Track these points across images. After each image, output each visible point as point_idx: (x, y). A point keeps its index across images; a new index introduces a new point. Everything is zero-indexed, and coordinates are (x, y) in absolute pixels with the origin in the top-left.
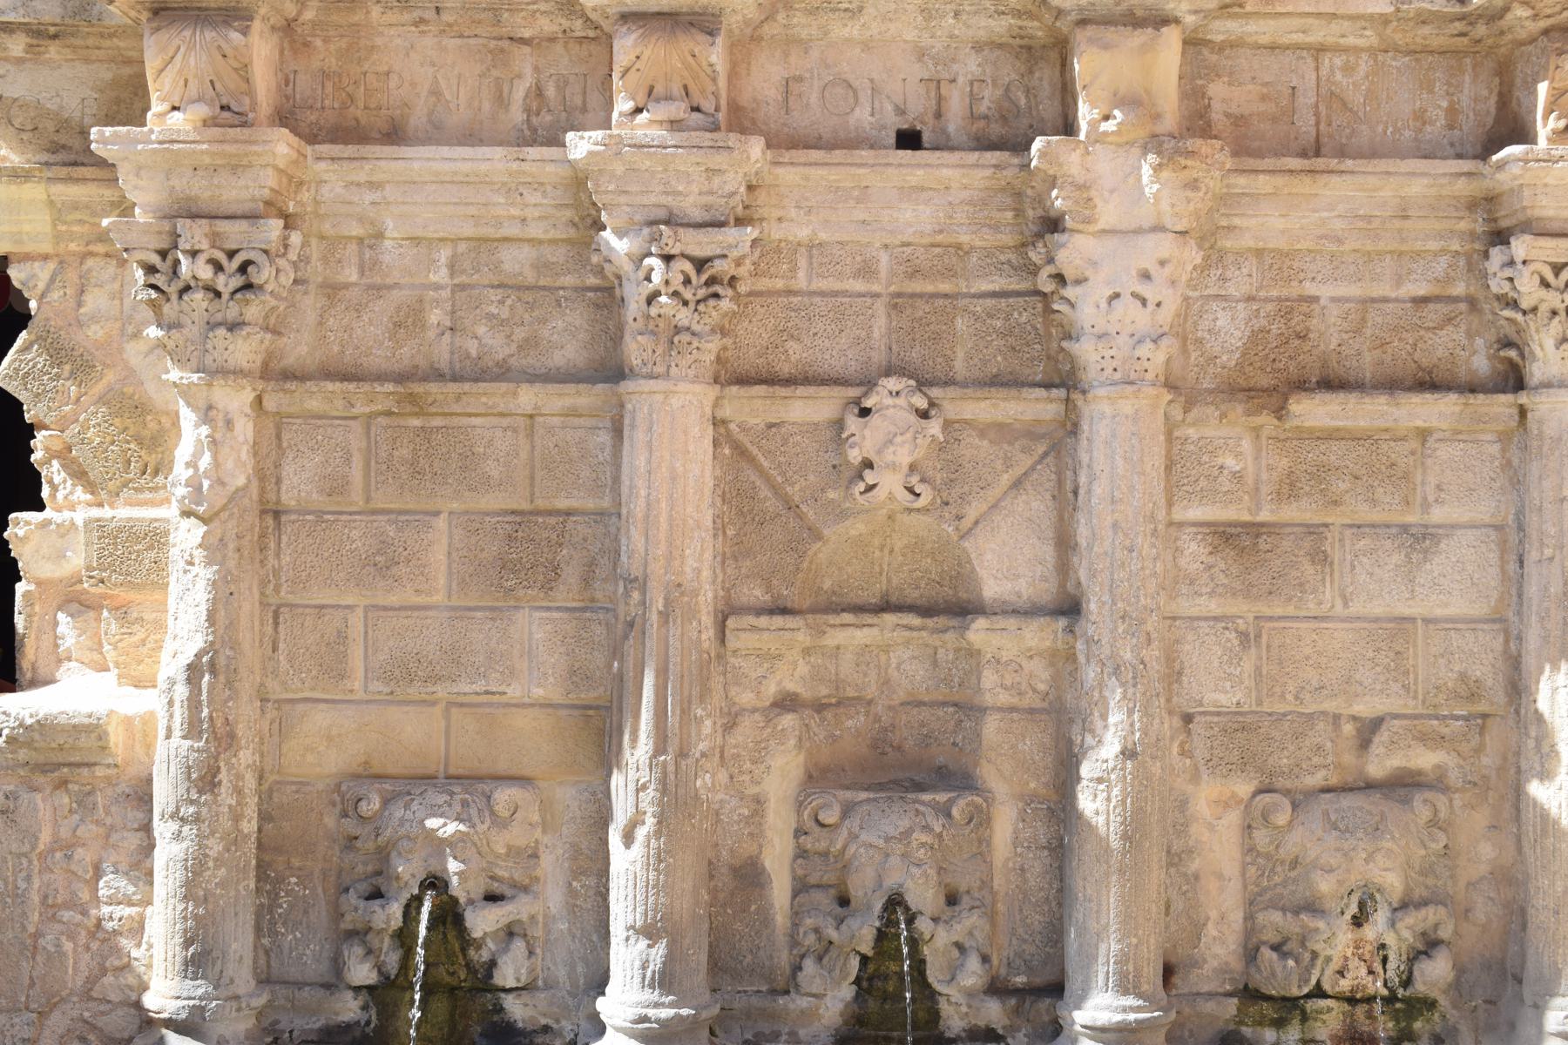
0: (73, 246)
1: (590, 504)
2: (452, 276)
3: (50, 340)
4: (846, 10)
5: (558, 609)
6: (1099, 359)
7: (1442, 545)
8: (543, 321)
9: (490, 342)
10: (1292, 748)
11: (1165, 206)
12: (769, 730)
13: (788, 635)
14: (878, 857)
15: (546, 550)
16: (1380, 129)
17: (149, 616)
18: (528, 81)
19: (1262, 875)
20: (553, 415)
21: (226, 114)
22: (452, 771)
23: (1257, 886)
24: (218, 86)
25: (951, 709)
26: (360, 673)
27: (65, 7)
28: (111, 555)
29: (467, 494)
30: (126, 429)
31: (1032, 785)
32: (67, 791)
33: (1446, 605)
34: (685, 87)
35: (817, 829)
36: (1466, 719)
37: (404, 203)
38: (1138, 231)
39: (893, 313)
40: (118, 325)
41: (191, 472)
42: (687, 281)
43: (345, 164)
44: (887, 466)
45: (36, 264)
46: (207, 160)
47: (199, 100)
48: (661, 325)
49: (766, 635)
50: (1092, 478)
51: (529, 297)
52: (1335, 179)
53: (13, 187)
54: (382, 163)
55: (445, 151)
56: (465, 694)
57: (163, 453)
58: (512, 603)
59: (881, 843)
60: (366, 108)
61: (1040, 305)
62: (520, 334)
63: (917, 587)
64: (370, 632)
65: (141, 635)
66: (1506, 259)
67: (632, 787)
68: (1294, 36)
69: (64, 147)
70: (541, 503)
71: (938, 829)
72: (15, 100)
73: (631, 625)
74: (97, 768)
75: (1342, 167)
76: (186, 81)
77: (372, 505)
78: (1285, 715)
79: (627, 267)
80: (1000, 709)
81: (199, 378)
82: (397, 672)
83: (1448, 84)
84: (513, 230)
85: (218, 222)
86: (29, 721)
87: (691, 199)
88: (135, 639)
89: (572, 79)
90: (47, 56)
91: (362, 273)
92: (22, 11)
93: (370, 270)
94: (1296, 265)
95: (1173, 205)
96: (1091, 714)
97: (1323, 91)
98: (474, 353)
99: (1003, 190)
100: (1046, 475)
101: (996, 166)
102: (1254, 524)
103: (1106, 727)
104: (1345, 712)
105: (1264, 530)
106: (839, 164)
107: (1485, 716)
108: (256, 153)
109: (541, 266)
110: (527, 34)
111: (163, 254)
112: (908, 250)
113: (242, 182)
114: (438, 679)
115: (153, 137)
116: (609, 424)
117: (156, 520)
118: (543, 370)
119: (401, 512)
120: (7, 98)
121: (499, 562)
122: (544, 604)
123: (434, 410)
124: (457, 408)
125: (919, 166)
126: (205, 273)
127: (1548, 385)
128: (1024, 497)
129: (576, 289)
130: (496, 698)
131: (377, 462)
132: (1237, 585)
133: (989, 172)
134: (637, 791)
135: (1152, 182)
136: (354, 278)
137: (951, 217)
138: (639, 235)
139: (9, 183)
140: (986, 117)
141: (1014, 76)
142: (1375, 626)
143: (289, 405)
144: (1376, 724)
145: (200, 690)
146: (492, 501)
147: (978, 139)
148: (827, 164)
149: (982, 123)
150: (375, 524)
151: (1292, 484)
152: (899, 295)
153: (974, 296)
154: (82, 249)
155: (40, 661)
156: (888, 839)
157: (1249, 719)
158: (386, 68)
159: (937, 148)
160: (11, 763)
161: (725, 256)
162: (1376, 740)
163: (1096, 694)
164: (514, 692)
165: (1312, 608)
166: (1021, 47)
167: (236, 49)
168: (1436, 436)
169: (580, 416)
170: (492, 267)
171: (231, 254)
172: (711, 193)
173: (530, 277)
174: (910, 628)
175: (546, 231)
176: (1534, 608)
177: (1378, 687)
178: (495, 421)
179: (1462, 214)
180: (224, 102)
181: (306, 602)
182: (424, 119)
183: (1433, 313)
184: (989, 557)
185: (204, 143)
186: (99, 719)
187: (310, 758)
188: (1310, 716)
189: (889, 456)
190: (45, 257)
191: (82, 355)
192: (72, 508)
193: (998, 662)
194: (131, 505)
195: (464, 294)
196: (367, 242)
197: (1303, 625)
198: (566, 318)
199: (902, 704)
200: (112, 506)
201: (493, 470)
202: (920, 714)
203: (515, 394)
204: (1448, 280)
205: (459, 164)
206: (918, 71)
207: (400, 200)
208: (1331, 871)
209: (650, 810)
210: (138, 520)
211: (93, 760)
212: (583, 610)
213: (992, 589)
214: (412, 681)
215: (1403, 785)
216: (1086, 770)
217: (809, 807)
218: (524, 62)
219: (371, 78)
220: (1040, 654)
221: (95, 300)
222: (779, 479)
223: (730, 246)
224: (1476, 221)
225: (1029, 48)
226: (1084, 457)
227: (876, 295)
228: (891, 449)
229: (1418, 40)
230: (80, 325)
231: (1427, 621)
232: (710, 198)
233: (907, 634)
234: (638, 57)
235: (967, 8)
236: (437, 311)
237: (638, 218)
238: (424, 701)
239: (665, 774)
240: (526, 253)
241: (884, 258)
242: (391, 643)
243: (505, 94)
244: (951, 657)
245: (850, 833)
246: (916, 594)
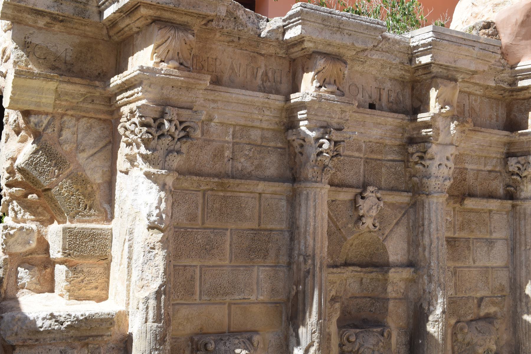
0: (60, 111)
1: (278, 227)
2: (233, 138)
3: (47, 150)
4: (362, 61)
5: (267, 266)
6: (435, 184)
7: (495, 245)
8: (263, 158)
9: (246, 165)
10: (464, 308)
11: (455, 138)
12: (332, 309)
13: (342, 274)
14: (371, 352)
15: (264, 244)
16: (482, 119)
17: (85, 270)
19: (459, 349)
20: (268, 194)
21: (182, 67)
22: (232, 330)
23: (458, 352)
24: (180, 55)
25: (368, 299)
26: (198, 293)
27: (75, 10)
28: (74, 243)
29: (239, 222)
30: (78, 190)
31: (401, 324)
32: (87, 348)
33: (496, 263)
34: (335, 80)
35: (348, 343)
36: (501, 297)
37: (224, 109)
38: (446, 145)
39: (366, 164)
40: (75, 145)
41: (158, 211)
43: (209, 92)
44: (370, 216)
45: (43, 116)
46: (180, 84)
47: (172, 59)
48: (320, 164)
49: (336, 275)
50: (430, 223)
51: (259, 149)
52: (480, 133)
53: (44, 82)
54: (222, 93)
55: (244, 92)
56: (236, 299)
57: (93, 200)
58: (251, 264)
59: (372, 347)
60: (208, 71)
61: (403, 165)
62: (256, 162)
63: (357, 258)
64: (203, 276)
65: (82, 278)
66: (517, 161)
67: (309, 333)
68: (466, 89)
69: (57, 68)
70: (263, 226)
71: (383, 341)
72: (37, 45)
73: (308, 272)
74: (104, 337)
75: (481, 130)
76: (169, 51)
77: (205, 226)
78: (462, 297)
79: (313, 142)
80: (392, 299)
81: (165, 172)
82: (213, 292)
83: (496, 108)
84: (257, 124)
85: (180, 110)
86: (81, 318)
87: (335, 120)
88: (79, 279)
89: (277, 71)
90: (53, 28)
91: (203, 134)
92: (57, 9)
93: (206, 133)
94: (464, 158)
95: (457, 137)
96: (432, 299)
97: (470, 106)
98: (240, 169)
99: (400, 127)
101: (402, 119)
102: (455, 238)
103: (437, 304)
104: (474, 296)
105: (456, 240)
106: (361, 113)
107: (505, 296)
108: (201, 84)
109: (263, 138)
110: (263, 52)
111: (155, 120)
112: (371, 144)
113: (190, 95)
114: (226, 294)
115: (163, 72)
116: (285, 198)
117: (94, 229)
118: (263, 177)
119: (214, 229)
120: (33, 44)
121: (249, 249)
122: (262, 264)
123: (229, 189)
124: (237, 189)
125: (382, 116)
127: (526, 199)
128: (400, 228)
129: (274, 147)
130: (245, 301)
131: (207, 209)
132: (451, 257)
133: (400, 121)
134: (312, 334)
135: (454, 130)
136: (200, 136)
137: (386, 134)
138: (319, 131)
139: (44, 80)
140: (392, 102)
141: (399, 90)
142: (482, 269)
143: (177, 184)
144: (481, 300)
145: (160, 302)
146: (246, 225)
147: (390, 109)
148: (358, 112)
149: (391, 104)
150: (206, 233)
151: (463, 226)
152: (367, 158)
153: (386, 161)
154: (63, 112)
155: (8, 289)
156: (374, 345)
157: (454, 299)
158: (214, 57)
160: (64, 337)
161: (343, 141)
162: (482, 304)
163: (434, 293)
164: (253, 298)
165: (467, 264)
166: (401, 81)
167: (190, 41)
168: (494, 212)
169: (276, 194)
170: (247, 136)
171: (181, 123)
172: (342, 119)
173: (259, 142)
174: (357, 272)
175: (268, 126)
176: (524, 264)
177: (483, 288)
178: (249, 195)
179: (501, 147)
180: (181, 61)
181: (179, 264)
182: (228, 78)
183: (493, 175)
184: (390, 247)
185: (182, 77)
186: (113, 316)
187: (180, 328)
188: (468, 298)
189: (371, 214)
190: (47, 114)
191: (61, 157)
192: (24, 221)
193: (393, 283)
194: (80, 222)
195: (238, 146)
196: (205, 122)
197: (466, 269)
198: (271, 158)
199: (350, 298)
200: (71, 222)
201: (248, 213)
202: (357, 301)
203: (258, 185)
204: (495, 166)
205: (248, 97)
206: (374, 84)
207: (223, 108)
208: (481, 346)
209: (316, 341)
210: (86, 228)
211: (101, 334)
212: (276, 266)
213: (392, 258)
214: (218, 295)
215: (489, 318)
216: (431, 318)
217: (346, 336)
218: (262, 62)
219: (210, 59)
220: (403, 280)
221: (66, 134)
222: (335, 220)
223: (347, 138)
224: (505, 149)
225: (403, 82)
226: (426, 216)
227: (361, 158)
228: (372, 211)
229: (491, 95)
230: (60, 144)
231: (492, 268)
232: (341, 120)
233: (356, 273)
234: (324, 68)
236: (228, 152)
237: (318, 125)
238: (221, 303)
239: (321, 326)
240: (258, 133)
241: (364, 145)
242: (211, 280)
243: (255, 73)
244: (368, 281)
245: (360, 343)
246: (356, 259)
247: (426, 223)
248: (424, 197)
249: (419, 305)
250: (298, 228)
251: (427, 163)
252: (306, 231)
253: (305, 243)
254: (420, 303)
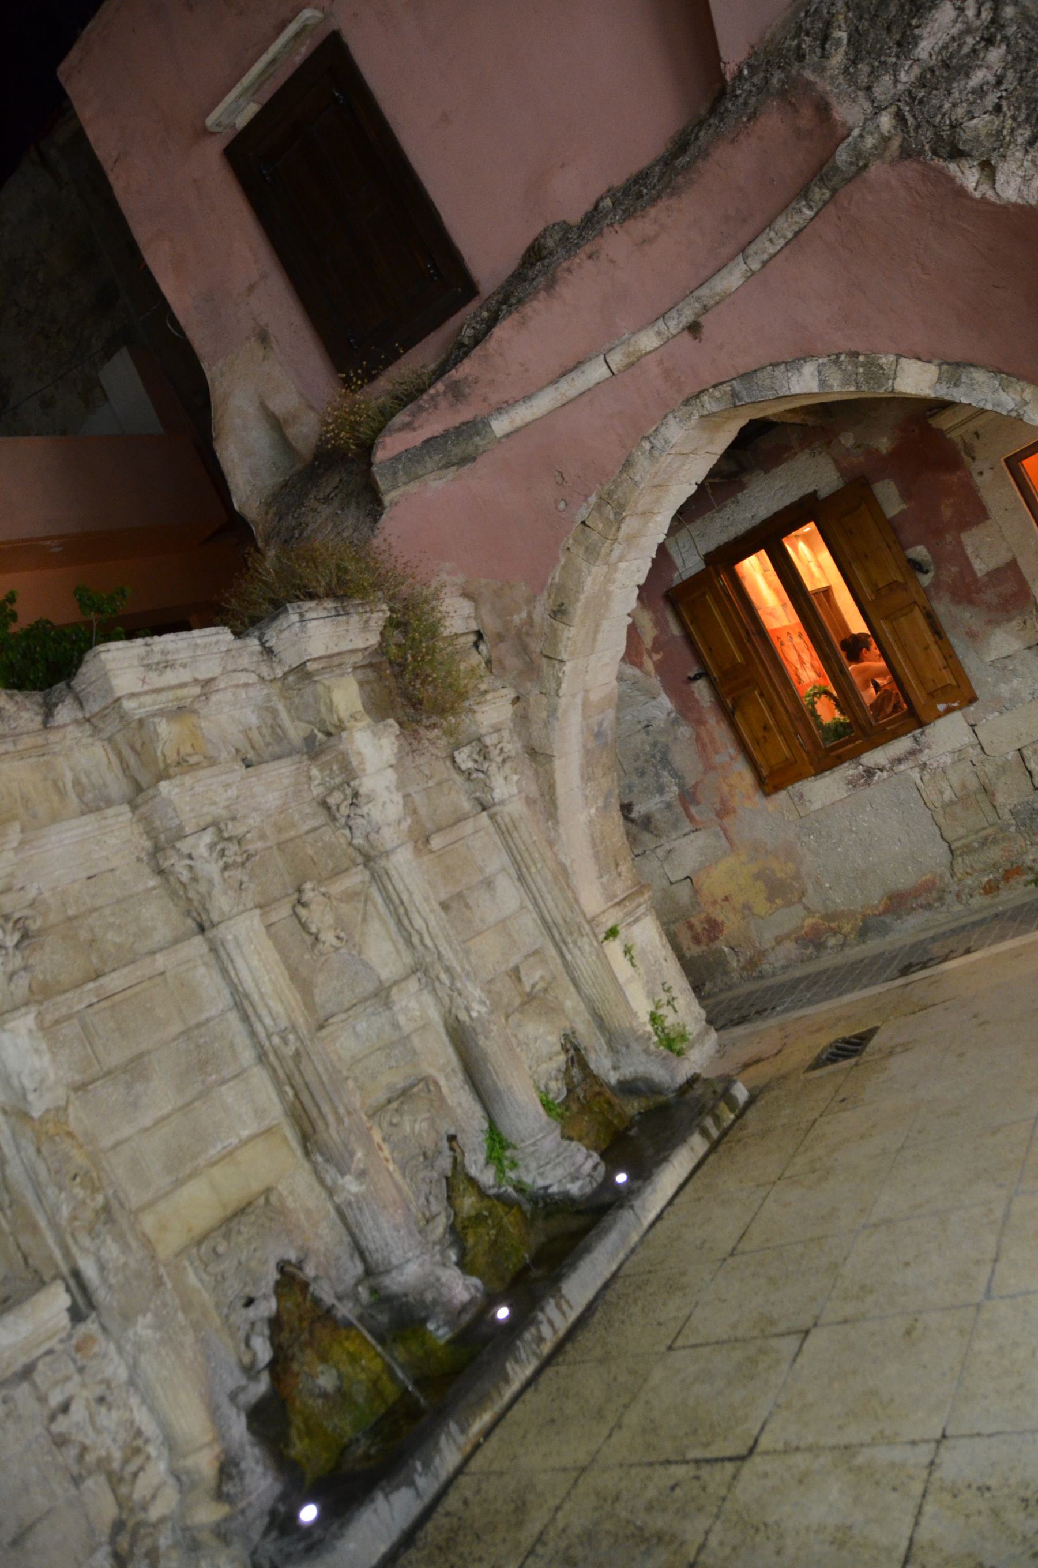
18: (69, 777)
73: (297, 1054)
152: (279, 844)
226: (400, 887)
227: (271, 847)
247: (405, 897)
248: (383, 862)
249: (451, 1021)
250: (247, 996)
251: (365, 810)
252: (262, 995)
253: (270, 1013)
254: (453, 1017)
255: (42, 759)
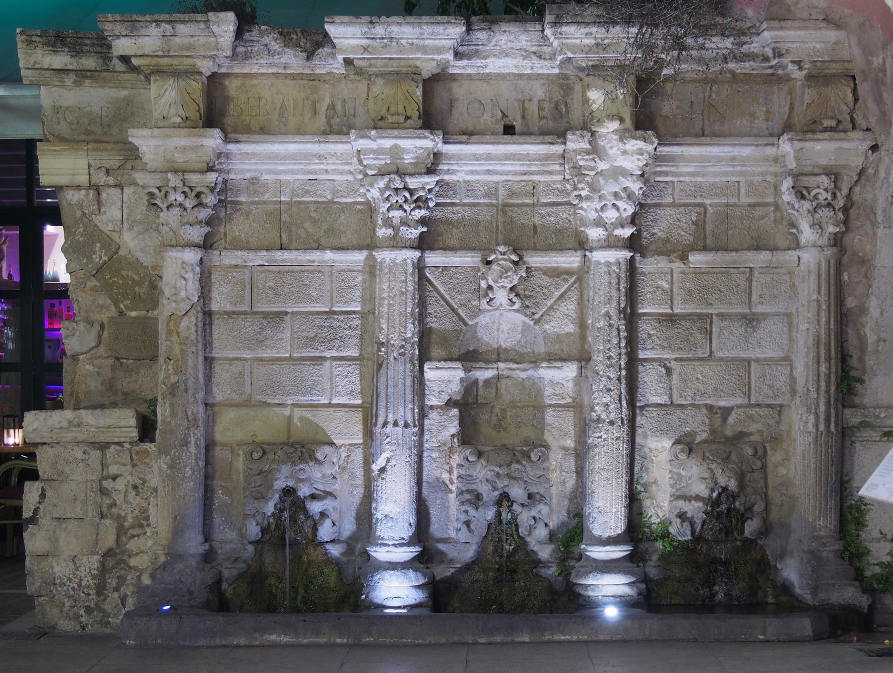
18: (327, 101)
42: (406, 201)
100: (574, 295)
126: (180, 198)
149: (544, 121)
159: (523, 134)
219: (252, 100)
235: (538, 65)
255: (311, 83)
